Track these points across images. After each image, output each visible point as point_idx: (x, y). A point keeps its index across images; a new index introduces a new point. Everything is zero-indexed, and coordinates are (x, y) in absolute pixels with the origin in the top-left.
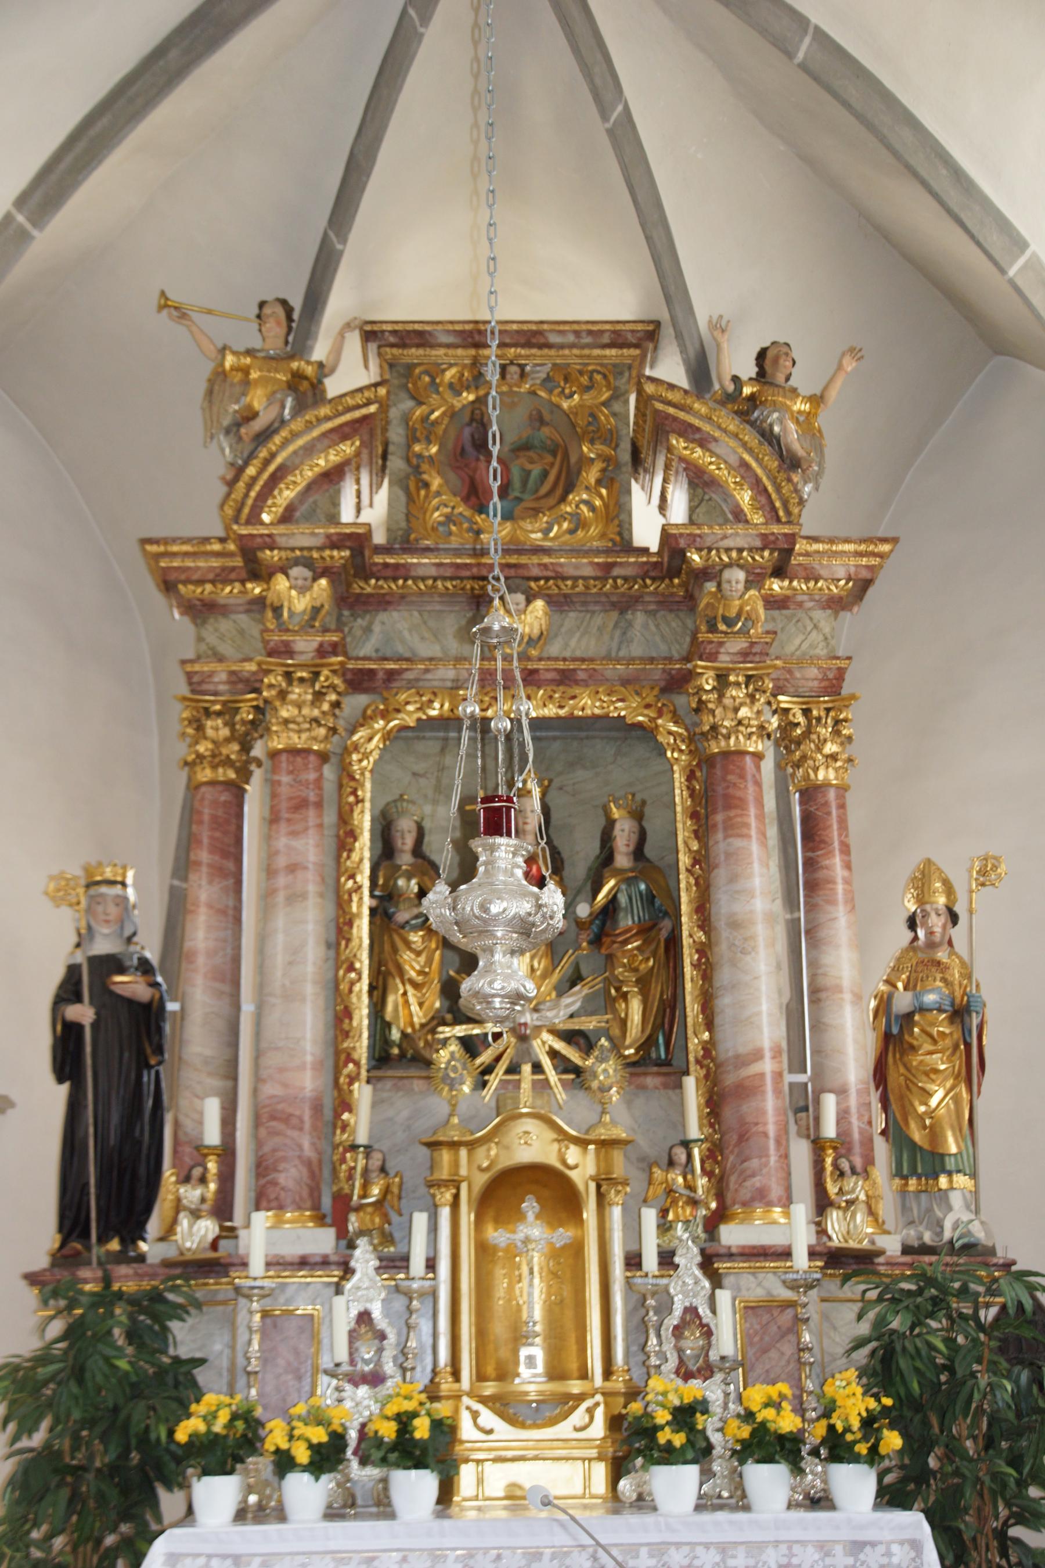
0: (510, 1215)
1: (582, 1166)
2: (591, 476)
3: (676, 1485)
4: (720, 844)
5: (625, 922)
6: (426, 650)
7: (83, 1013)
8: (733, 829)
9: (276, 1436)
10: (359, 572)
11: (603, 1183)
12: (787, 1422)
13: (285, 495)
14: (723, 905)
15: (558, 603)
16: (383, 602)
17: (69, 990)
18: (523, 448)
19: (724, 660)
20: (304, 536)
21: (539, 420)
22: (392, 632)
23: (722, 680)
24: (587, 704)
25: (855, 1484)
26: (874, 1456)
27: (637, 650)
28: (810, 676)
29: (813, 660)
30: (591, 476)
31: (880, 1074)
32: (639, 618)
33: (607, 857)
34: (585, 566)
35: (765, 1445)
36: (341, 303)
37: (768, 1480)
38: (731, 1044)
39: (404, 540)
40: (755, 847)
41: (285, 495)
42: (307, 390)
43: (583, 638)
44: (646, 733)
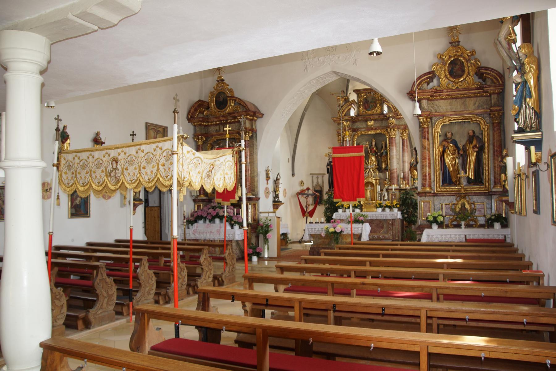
0: (368, 186)
1: (374, 182)
2: (378, 105)
3: (380, 210)
4: (391, 147)
5: (384, 155)
6: (362, 127)
7: (329, 167)
8: (392, 146)
9: (345, 206)
10: (353, 120)
11: (376, 183)
12: (389, 204)
13: (345, 112)
14: (391, 154)
15: (375, 120)
16: (356, 122)
17: (328, 165)
18: (371, 102)
19: (391, 127)
20: (346, 118)
21: (373, 99)
22: (358, 125)
23: (390, 130)
24: (378, 132)
25: (396, 210)
26: (396, 207)
27: (384, 125)
28: (402, 127)
29: (402, 125)
30: (378, 105)
31: (410, 170)
32: (384, 121)
33: (382, 147)
34: (376, 117)
35: (387, 206)
36: (350, 87)
37: (387, 210)
38: (392, 169)
39: (358, 115)
40: (394, 148)
41: (345, 112)
42: (347, 100)
43: (378, 124)
44: (384, 135)
